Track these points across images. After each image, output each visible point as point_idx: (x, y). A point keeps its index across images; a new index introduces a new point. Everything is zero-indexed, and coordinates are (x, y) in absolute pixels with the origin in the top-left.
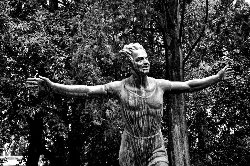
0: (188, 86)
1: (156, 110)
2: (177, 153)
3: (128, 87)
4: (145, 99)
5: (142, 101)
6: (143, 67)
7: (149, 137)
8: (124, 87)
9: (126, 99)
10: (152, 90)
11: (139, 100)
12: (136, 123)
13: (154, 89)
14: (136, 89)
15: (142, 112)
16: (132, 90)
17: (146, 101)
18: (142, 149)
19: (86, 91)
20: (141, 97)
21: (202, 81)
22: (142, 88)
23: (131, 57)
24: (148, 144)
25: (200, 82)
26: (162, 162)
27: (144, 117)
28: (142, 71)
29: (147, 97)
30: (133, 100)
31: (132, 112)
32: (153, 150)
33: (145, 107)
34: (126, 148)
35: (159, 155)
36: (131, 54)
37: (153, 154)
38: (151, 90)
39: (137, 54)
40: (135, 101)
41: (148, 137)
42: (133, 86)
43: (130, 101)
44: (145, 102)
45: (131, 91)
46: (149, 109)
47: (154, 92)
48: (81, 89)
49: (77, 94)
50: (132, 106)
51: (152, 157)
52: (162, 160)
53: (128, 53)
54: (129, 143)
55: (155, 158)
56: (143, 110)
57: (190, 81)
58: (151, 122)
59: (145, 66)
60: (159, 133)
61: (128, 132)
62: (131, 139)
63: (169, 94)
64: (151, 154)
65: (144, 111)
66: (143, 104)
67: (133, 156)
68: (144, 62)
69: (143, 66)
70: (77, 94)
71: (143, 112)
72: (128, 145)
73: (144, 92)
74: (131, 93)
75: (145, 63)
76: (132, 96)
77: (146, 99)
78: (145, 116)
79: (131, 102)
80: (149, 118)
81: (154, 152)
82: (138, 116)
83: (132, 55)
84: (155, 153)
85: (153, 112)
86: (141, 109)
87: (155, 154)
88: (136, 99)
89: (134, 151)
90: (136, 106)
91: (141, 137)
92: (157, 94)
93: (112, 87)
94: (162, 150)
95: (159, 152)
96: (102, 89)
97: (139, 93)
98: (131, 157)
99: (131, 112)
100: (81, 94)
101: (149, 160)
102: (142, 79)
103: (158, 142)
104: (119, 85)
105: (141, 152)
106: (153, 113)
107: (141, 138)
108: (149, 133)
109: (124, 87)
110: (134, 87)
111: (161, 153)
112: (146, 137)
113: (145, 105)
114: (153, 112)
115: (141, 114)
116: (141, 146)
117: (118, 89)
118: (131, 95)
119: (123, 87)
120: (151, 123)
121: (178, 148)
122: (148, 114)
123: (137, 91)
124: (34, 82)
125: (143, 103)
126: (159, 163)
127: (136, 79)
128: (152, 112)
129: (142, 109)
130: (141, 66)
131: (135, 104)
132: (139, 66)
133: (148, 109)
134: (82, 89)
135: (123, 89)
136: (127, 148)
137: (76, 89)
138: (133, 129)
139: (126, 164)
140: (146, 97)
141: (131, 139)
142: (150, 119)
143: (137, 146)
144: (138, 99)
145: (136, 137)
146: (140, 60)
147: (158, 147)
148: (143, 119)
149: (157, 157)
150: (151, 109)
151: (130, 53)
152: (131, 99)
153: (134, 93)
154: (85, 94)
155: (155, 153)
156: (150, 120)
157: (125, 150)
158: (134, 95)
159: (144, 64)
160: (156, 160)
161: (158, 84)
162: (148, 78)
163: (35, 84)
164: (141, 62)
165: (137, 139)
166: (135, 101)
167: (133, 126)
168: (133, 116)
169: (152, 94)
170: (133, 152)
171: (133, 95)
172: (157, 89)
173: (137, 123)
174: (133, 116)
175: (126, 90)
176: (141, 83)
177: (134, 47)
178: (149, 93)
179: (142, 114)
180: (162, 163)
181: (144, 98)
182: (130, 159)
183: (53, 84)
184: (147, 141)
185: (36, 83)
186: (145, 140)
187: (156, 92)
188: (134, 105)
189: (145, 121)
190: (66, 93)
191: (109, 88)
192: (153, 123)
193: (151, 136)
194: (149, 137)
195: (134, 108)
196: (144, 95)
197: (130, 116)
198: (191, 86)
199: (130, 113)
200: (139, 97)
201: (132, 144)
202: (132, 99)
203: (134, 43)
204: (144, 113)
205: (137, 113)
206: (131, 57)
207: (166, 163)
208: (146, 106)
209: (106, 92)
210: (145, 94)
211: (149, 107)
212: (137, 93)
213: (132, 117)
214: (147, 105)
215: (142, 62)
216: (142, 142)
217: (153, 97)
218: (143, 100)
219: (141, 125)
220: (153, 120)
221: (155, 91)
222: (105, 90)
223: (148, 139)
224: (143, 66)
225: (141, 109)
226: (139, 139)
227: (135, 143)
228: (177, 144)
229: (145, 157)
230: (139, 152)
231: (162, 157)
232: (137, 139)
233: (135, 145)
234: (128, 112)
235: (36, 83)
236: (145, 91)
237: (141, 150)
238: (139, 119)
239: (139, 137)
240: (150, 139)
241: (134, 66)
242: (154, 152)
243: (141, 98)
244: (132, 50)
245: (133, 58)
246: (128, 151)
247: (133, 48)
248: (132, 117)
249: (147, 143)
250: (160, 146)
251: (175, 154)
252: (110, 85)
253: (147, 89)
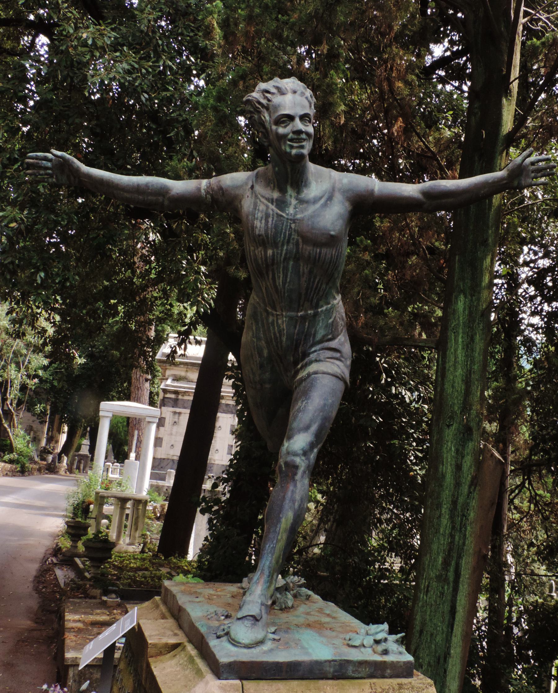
0: (420, 196)
1: (318, 250)
2: (451, 363)
3: (259, 189)
4: (291, 220)
5: (283, 224)
6: (291, 140)
7: (299, 314)
8: (252, 187)
9: (250, 217)
10: (315, 201)
11: (276, 221)
12: (268, 277)
13: (321, 198)
14: (276, 195)
15: (282, 250)
16: (267, 196)
17: (293, 226)
18: (284, 339)
19: (163, 192)
20: (284, 215)
21: (459, 187)
22: (290, 191)
23: (266, 115)
24: (299, 330)
25: (454, 188)
26: (324, 373)
27: (288, 264)
28: (288, 150)
29: (299, 216)
30: (263, 221)
31: (260, 249)
32: (309, 345)
33: (291, 241)
34: (251, 334)
35: (322, 358)
36: (266, 105)
37: (310, 354)
38: (312, 200)
39: (279, 106)
41: (298, 312)
42: (272, 185)
43: (257, 223)
44: (291, 227)
45: (263, 200)
46: (301, 247)
47: (318, 205)
48: (150, 185)
49: (141, 197)
50: (259, 235)
51: (307, 360)
52: (325, 370)
53: (259, 103)
54: (257, 323)
55: (311, 362)
56: (285, 248)
57: (428, 184)
58: (305, 276)
59: (296, 137)
60: (329, 306)
62: (261, 315)
63: (363, 209)
64: (306, 355)
65: (287, 250)
66: (285, 233)
67: (265, 352)
68: (294, 126)
69: (289, 137)
70: (141, 197)
71: (284, 252)
72: (254, 328)
73: (294, 202)
74: (263, 203)
75: (295, 129)
76: (262, 212)
77: (294, 221)
78: (291, 263)
80: (301, 267)
81: (313, 349)
82: (273, 260)
83: (267, 108)
84: (315, 351)
85: (310, 253)
86: (280, 244)
87: (315, 353)
88: (270, 220)
89: (267, 342)
90: (267, 236)
91: (282, 311)
92: (328, 209)
93: (223, 186)
94: (333, 346)
95: (326, 351)
96: (199, 189)
97: (281, 204)
98: (260, 354)
99: (258, 248)
100: (149, 198)
101: (299, 366)
102: (289, 170)
103: (326, 326)
104: (239, 183)
105: (281, 347)
106: (309, 257)
107: (282, 315)
108: (302, 303)
109: (252, 187)
110: (273, 189)
111: (330, 354)
112: (293, 311)
113: (290, 235)
114: (310, 253)
115: (279, 256)
116: (280, 332)
117: (237, 192)
119: (250, 186)
120: (304, 279)
121: (456, 350)
122: (297, 257)
123: (277, 200)
124: (44, 162)
125: (286, 230)
126: (316, 375)
127: (277, 169)
128: (307, 253)
129: (283, 245)
130: (284, 136)
132: (282, 138)
133: (297, 244)
134: (153, 185)
135: (248, 193)
136: (253, 335)
137: (138, 185)
139: (252, 369)
140: (296, 214)
142: (301, 270)
143: (272, 331)
144: (275, 219)
145: (270, 310)
146: (283, 122)
147: (326, 339)
148: (286, 269)
149: (316, 361)
150: (304, 246)
151: (264, 102)
152: (259, 218)
153: (270, 204)
154: (161, 199)
155: (315, 351)
156: (304, 273)
157: (249, 338)
158: (267, 207)
159: (294, 132)
160: (313, 367)
161: (338, 185)
162: (312, 167)
163: (46, 168)
164: (285, 127)
165: (273, 315)
167: (264, 283)
168: (262, 258)
169: (312, 209)
170: (265, 345)
171: (264, 208)
172: (330, 198)
173: (271, 276)
174: (262, 258)
175: (254, 195)
176: (290, 181)
177: (278, 88)
178: (305, 205)
179: (281, 255)
180: (325, 375)
181: (290, 217)
182: (258, 359)
183: (84, 168)
184: (296, 323)
185: (49, 164)
186: (291, 318)
187: (325, 205)
189: (289, 274)
190: (115, 192)
191: (216, 188)
192: (309, 280)
193: (306, 311)
194: (299, 314)
195: (263, 240)
196: (291, 210)
198: (428, 194)
199: (256, 252)
200: (277, 214)
202: (262, 218)
203: (281, 78)
204: (286, 254)
205: (270, 252)
206: (266, 116)
207: (334, 378)
208: (293, 237)
209: (208, 196)
210: (295, 208)
211: (300, 240)
212: (275, 204)
213: (260, 261)
214: (295, 236)
215: (288, 128)
216: (283, 323)
217: (312, 216)
218: (287, 222)
219: (279, 282)
220: (310, 272)
221: (322, 201)
222: (207, 193)
223: (297, 316)
224: (289, 137)
225: (280, 244)
226: (277, 315)
228: (456, 341)
229: (292, 359)
230: (277, 346)
231: (327, 363)
232: (273, 315)
233: (269, 328)
234: (252, 248)
235: (49, 164)
236: (297, 199)
237: (281, 341)
238: (275, 267)
239: (276, 311)
240: (304, 318)
242: (313, 349)
243: (281, 216)
244: (268, 95)
245: (270, 117)
246: (255, 340)
247: (273, 90)
248: (260, 261)
249: (295, 328)
250: (330, 336)
251: (447, 366)
252: (220, 181)
253: (303, 196)
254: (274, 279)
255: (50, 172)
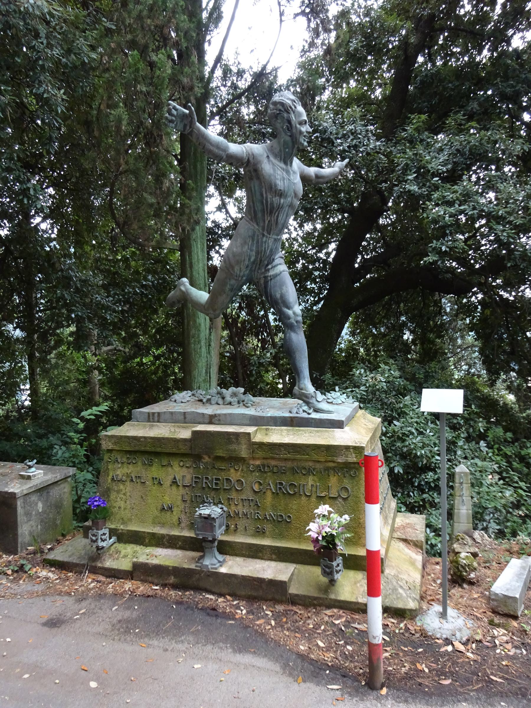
2: (196, 260)
34: (247, 247)
40: (284, 183)
53: (291, 107)
54: (253, 240)
55: (277, 265)
61: (255, 225)
62: (258, 236)
67: (252, 259)
79: (279, 183)
83: (294, 113)
101: (270, 267)
118: (279, 172)
121: (197, 252)
131: (284, 188)
138: (267, 222)
141: (258, 236)
166: (284, 183)
188: (282, 188)
197: (272, 204)
201: (258, 242)
219: (280, 218)
227: (262, 242)
228: (197, 248)
234: (269, 196)
241: (294, 131)
251: (193, 261)
254: (278, 217)
255: (174, 118)
